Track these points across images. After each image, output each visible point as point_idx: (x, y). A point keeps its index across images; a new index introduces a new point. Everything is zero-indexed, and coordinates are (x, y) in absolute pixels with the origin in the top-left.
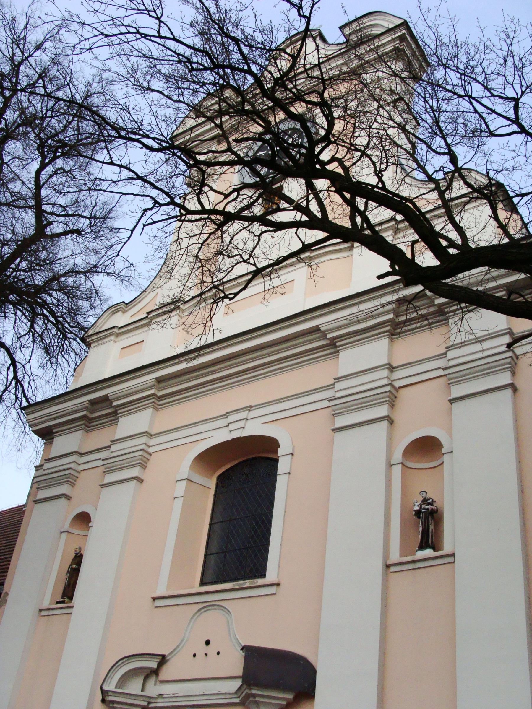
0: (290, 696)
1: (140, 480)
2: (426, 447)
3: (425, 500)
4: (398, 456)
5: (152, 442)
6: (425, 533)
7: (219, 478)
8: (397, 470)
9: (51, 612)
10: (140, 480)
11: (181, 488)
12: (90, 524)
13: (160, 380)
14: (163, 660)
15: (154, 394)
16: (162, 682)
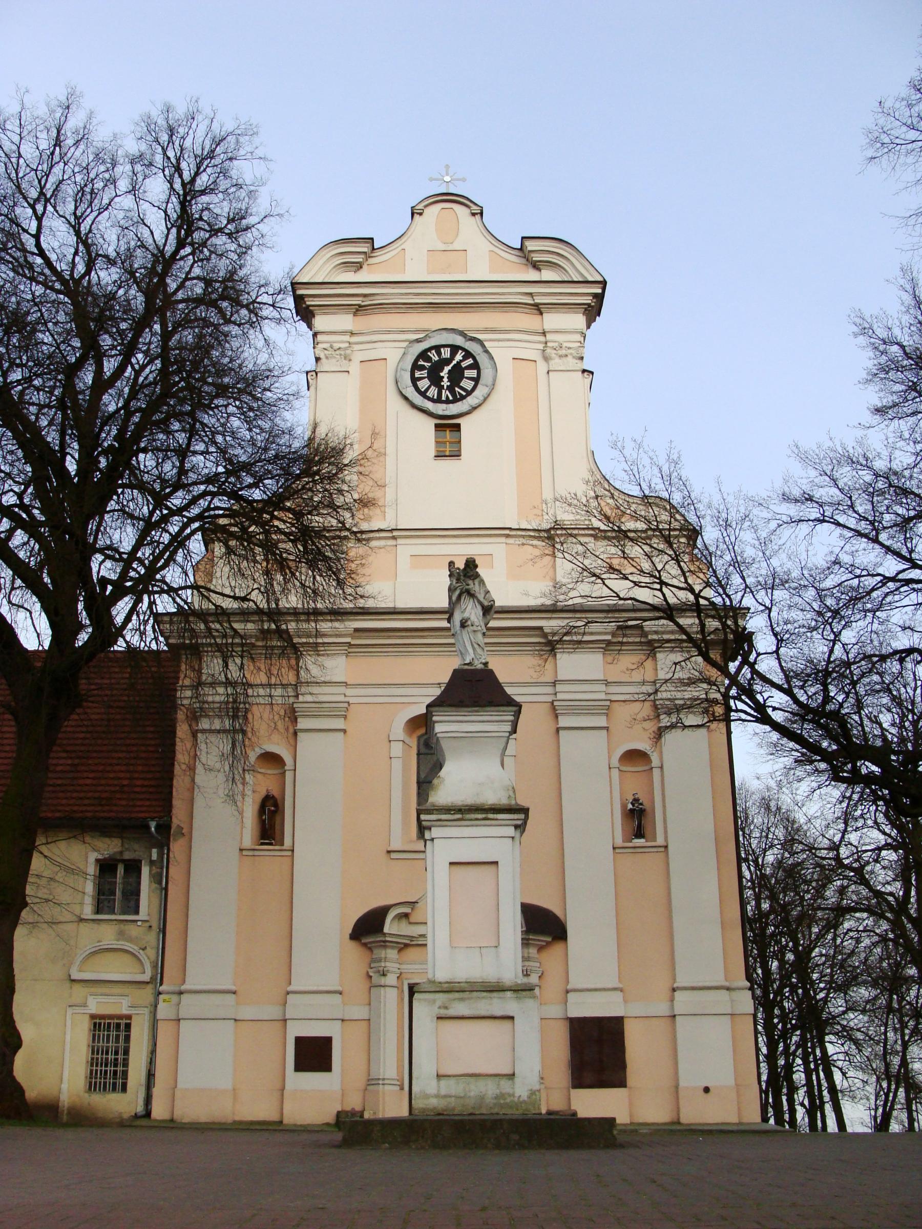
0: (549, 939)
1: (344, 731)
2: (634, 756)
3: (636, 800)
4: (615, 762)
5: (349, 692)
6: (640, 826)
7: (419, 738)
8: (615, 773)
9: (256, 853)
10: (344, 731)
11: (397, 749)
12: (286, 768)
13: (357, 630)
14: (413, 904)
15: (349, 643)
16: (410, 923)
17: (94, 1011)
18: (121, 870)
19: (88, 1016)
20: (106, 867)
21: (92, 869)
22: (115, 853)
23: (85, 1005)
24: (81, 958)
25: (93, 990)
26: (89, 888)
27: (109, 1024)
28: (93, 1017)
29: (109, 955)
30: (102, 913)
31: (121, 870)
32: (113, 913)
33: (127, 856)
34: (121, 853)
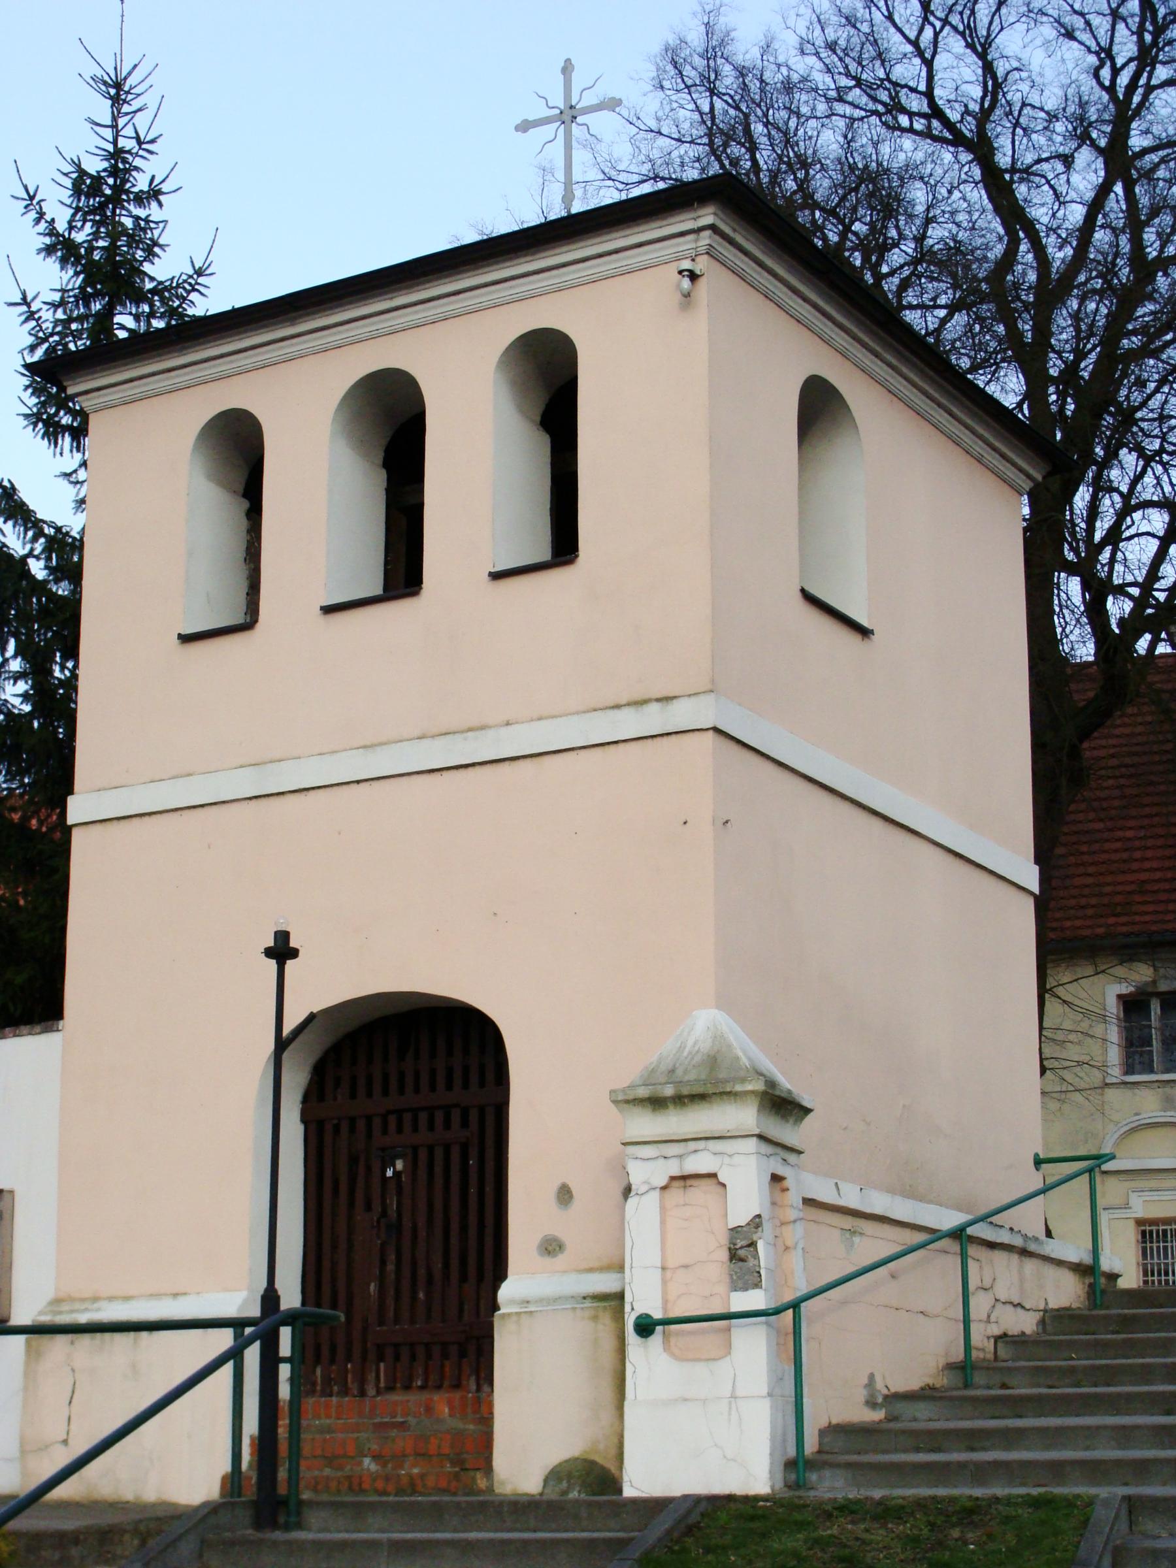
17: (1140, 1214)
18: (1155, 1007)
19: (1132, 1224)
20: (1134, 1005)
21: (1113, 1007)
22: (1146, 984)
23: (1127, 1206)
24: (1113, 1140)
25: (1133, 1184)
26: (1114, 1034)
27: (1165, 1231)
28: (1139, 1222)
29: (1150, 1134)
30: (1133, 1073)
31: (1155, 1007)
32: (1151, 1071)
33: (1163, 987)
34: (1154, 982)
